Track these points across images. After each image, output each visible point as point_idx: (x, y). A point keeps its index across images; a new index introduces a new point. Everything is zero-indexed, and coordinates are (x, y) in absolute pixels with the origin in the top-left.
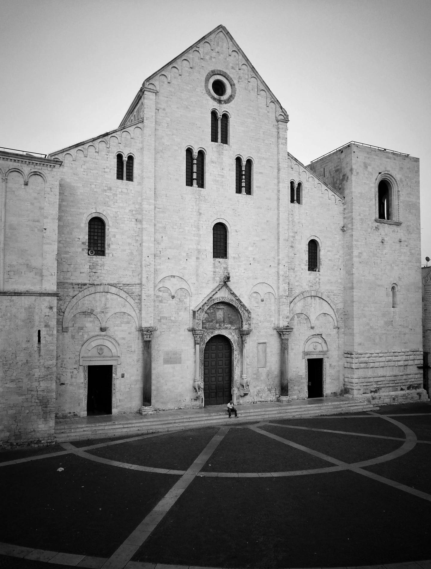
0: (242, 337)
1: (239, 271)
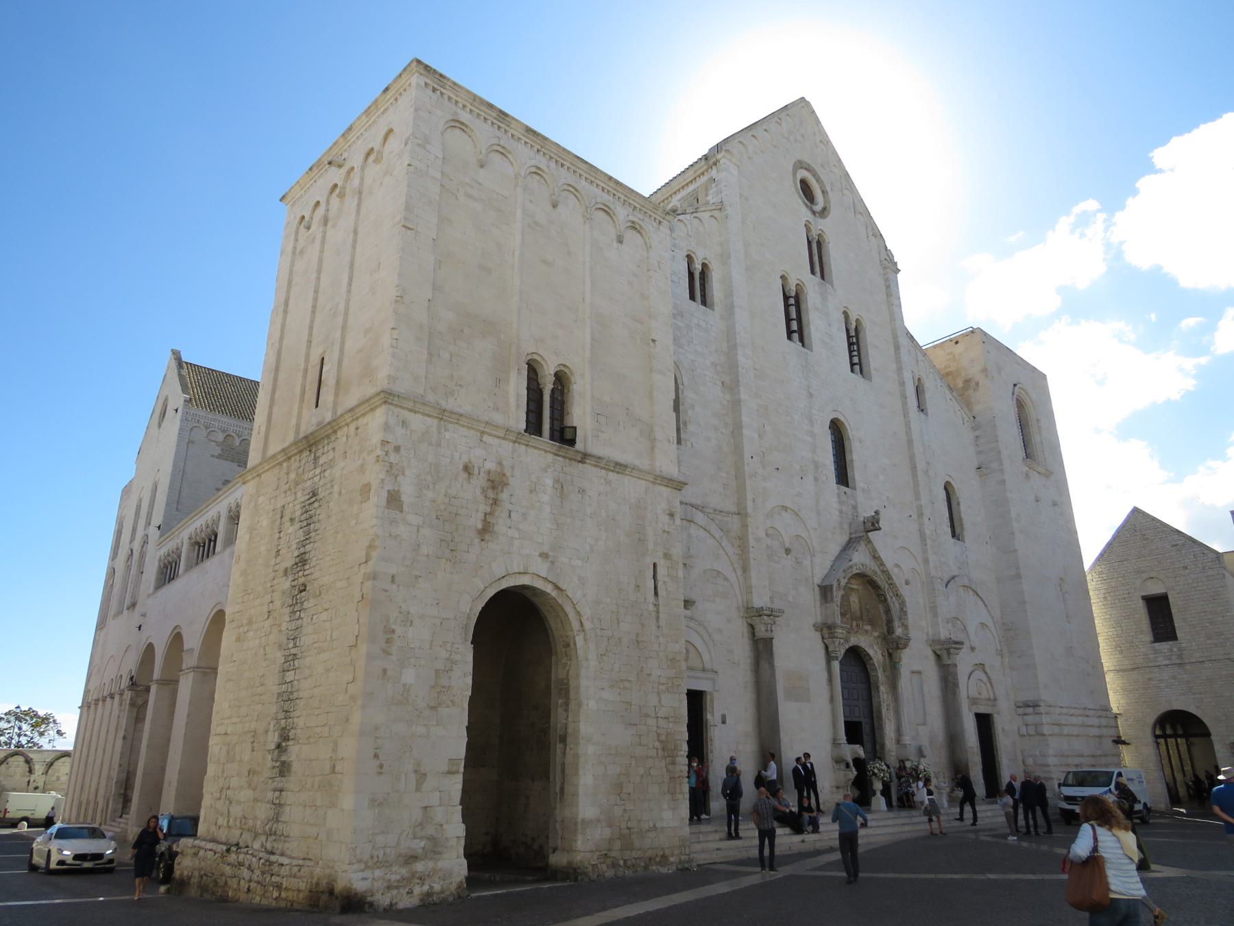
0: (890, 655)
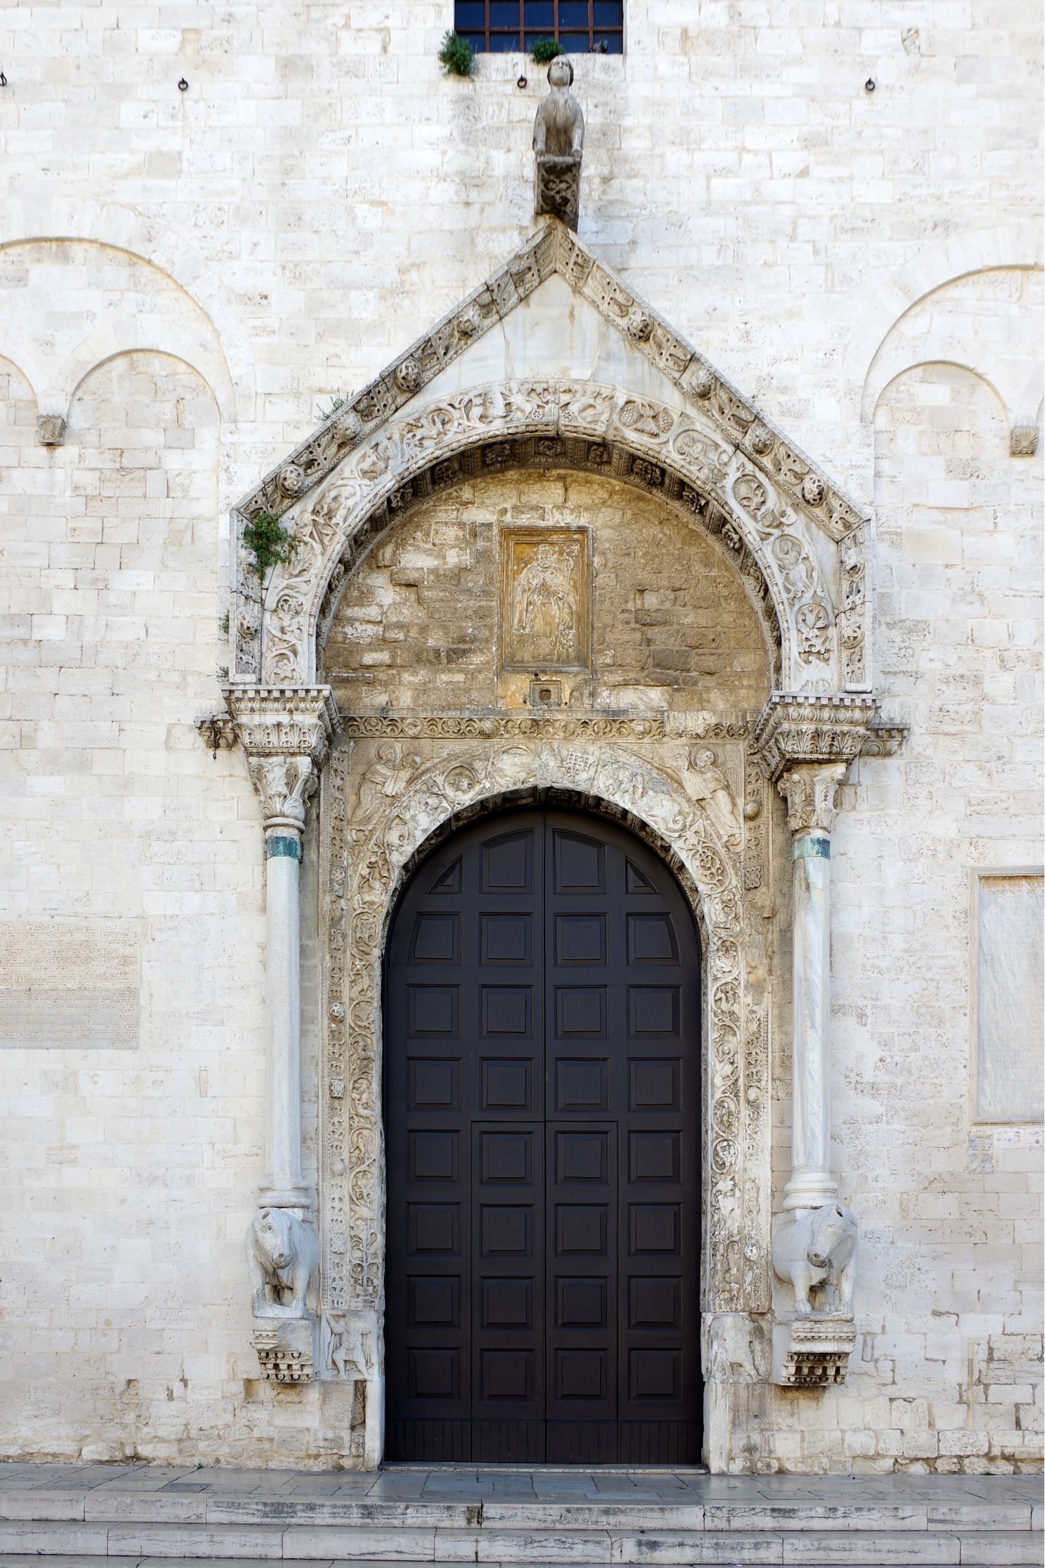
1: (747, 159)
